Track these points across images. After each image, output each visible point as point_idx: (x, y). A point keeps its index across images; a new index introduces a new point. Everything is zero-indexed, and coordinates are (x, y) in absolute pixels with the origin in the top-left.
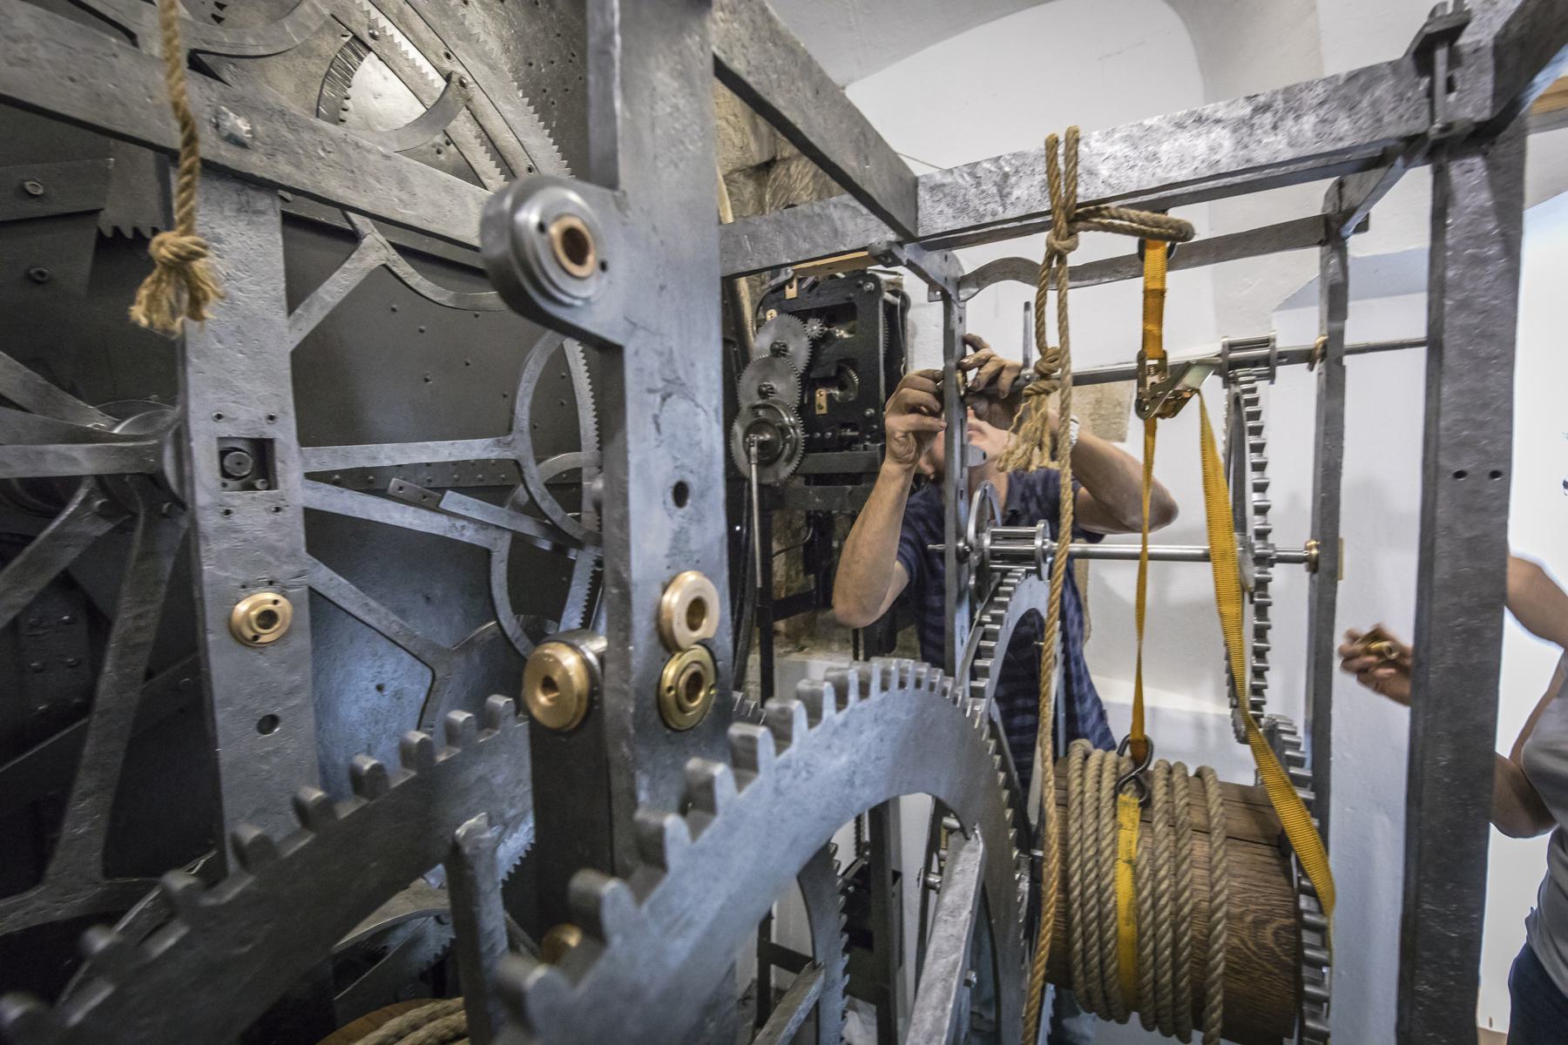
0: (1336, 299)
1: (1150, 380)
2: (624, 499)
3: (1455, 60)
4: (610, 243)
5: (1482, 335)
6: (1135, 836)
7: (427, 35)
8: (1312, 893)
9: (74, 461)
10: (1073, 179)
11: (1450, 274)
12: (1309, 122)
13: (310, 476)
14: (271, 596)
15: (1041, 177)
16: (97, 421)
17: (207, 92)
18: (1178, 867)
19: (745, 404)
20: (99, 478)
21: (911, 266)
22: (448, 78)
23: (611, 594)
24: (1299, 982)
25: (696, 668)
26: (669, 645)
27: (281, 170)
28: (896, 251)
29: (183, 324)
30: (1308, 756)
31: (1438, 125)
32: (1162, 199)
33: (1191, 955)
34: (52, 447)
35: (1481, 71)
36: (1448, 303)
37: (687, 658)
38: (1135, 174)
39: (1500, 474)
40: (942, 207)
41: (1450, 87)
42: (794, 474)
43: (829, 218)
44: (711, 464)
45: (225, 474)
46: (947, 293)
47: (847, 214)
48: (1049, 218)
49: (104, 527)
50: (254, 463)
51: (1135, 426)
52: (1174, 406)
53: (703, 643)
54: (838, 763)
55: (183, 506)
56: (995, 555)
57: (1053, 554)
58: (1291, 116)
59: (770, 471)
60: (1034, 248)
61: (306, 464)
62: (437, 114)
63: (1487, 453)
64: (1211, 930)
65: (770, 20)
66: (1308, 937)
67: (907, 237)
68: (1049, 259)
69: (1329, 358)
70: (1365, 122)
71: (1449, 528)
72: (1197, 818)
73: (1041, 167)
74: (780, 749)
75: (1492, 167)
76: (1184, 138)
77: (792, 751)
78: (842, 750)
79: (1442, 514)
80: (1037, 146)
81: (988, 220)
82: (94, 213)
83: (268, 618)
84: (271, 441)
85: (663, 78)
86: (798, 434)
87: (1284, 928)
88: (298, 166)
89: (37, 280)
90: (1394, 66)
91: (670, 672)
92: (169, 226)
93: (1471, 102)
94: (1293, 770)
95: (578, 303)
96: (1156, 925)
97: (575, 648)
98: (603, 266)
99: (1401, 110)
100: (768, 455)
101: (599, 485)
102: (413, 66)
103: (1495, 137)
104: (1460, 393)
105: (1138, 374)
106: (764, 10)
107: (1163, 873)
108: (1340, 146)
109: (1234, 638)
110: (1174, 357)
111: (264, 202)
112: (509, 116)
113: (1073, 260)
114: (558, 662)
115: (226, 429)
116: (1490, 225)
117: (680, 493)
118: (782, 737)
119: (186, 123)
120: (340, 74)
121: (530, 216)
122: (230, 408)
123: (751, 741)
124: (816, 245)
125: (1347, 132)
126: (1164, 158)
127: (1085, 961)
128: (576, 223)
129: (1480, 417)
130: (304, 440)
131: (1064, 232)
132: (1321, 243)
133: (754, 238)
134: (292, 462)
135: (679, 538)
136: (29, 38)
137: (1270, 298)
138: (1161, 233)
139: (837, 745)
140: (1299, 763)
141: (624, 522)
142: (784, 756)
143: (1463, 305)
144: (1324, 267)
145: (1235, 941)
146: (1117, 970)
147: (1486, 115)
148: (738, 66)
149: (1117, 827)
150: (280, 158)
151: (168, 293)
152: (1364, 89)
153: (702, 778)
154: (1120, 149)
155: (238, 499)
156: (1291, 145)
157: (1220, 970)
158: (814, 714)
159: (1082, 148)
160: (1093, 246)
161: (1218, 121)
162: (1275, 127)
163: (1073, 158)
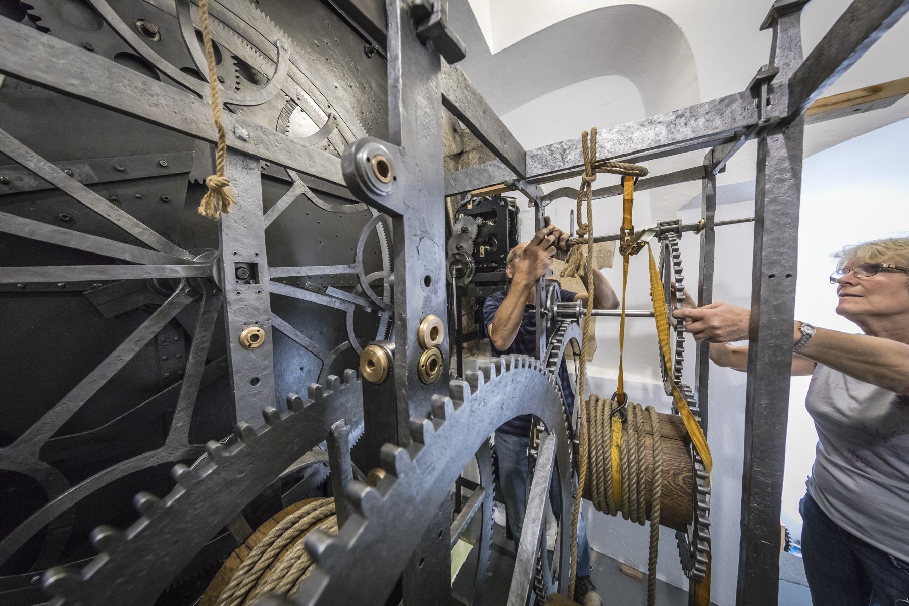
0: (710, 202)
1: (626, 238)
2: (404, 282)
3: (770, 90)
4: (397, 168)
5: (782, 214)
6: (620, 436)
7: (321, 98)
8: (701, 462)
9: (176, 271)
10: (594, 150)
11: (767, 187)
12: (702, 121)
13: (272, 279)
14: (257, 328)
15: (580, 150)
16: (187, 256)
17: (230, 118)
18: (639, 449)
19: (450, 253)
20: (187, 279)
21: (523, 191)
22: (329, 116)
23: (397, 326)
24: (696, 502)
25: (434, 357)
26: (422, 347)
27: (261, 151)
28: (516, 183)
29: (220, 214)
30: (698, 402)
31: (763, 120)
32: (636, 157)
33: (645, 488)
34: (168, 266)
35: (783, 95)
36: (766, 199)
37: (430, 353)
38: (622, 147)
39: (791, 276)
40: (537, 164)
41: (768, 103)
42: (471, 282)
43: (488, 170)
44: (440, 269)
45: (238, 277)
46: (536, 203)
47: (495, 169)
48: (583, 168)
49: (189, 300)
50: (249, 273)
51: (618, 259)
52: (638, 249)
53: (437, 346)
54: (495, 400)
55: (221, 291)
57: (585, 314)
58: (694, 118)
60: (575, 183)
61: (271, 273)
62: (325, 131)
63: (784, 266)
65: (465, 80)
66: (699, 481)
67: (521, 177)
68: (583, 186)
69: (706, 229)
71: (766, 300)
72: (647, 428)
73: (580, 145)
74: (473, 392)
75: (787, 138)
76: (644, 130)
77: (478, 392)
78: (499, 394)
79: (763, 293)
80: (578, 137)
81: (557, 169)
82: (188, 173)
83: (255, 337)
84: (257, 264)
85: (420, 99)
87: (687, 477)
88: (267, 150)
89: (164, 201)
90: (742, 95)
91: (423, 358)
92: (215, 173)
93: (778, 109)
94: (691, 408)
95: (384, 194)
96: (629, 474)
97: (382, 348)
98: (395, 179)
99: (745, 114)
100: (460, 274)
101: (392, 278)
102: (315, 111)
103: (788, 124)
104: (772, 240)
105: (621, 238)
106: (463, 75)
107: (632, 451)
108: (716, 131)
109: (665, 350)
110: (637, 230)
111: (253, 164)
112: (354, 131)
113: (595, 186)
114: (375, 353)
115: (238, 259)
116: (786, 164)
117: (427, 281)
118: (474, 387)
119: (220, 129)
120: (286, 114)
121: (363, 155)
122: (239, 250)
123: (461, 387)
124: (482, 182)
125: (719, 125)
126: (635, 139)
127: (598, 489)
128: (383, 159)
130: (271, 263)
131: (590, 173)
132: (703, 178)
133: (455, 180)
134: (266, 273)
135: (427, 300)
136: (158, 95)
137: (681, 202)
138: (632, 174)
139: (495, 392)
140: (694, 405)
141: (403, 292)
142: (474, 395)
143: (773, 201)
144: (704, 188)
145: (665, 482)
146: (612, 493)
147: (785, 114)
148: (451, 98)
149: (612, 431)
150: (260, 146)
151: (213, 201)
152: (727, 106)
153: (439, 404)
154: (615, 136)
155: (243, 287)
156: (693, 132)
158: (487, 377)
159: (598, 136)
160: (603, 180)
161: (659, 123)
162: (686, 124)
163: (594, 141)
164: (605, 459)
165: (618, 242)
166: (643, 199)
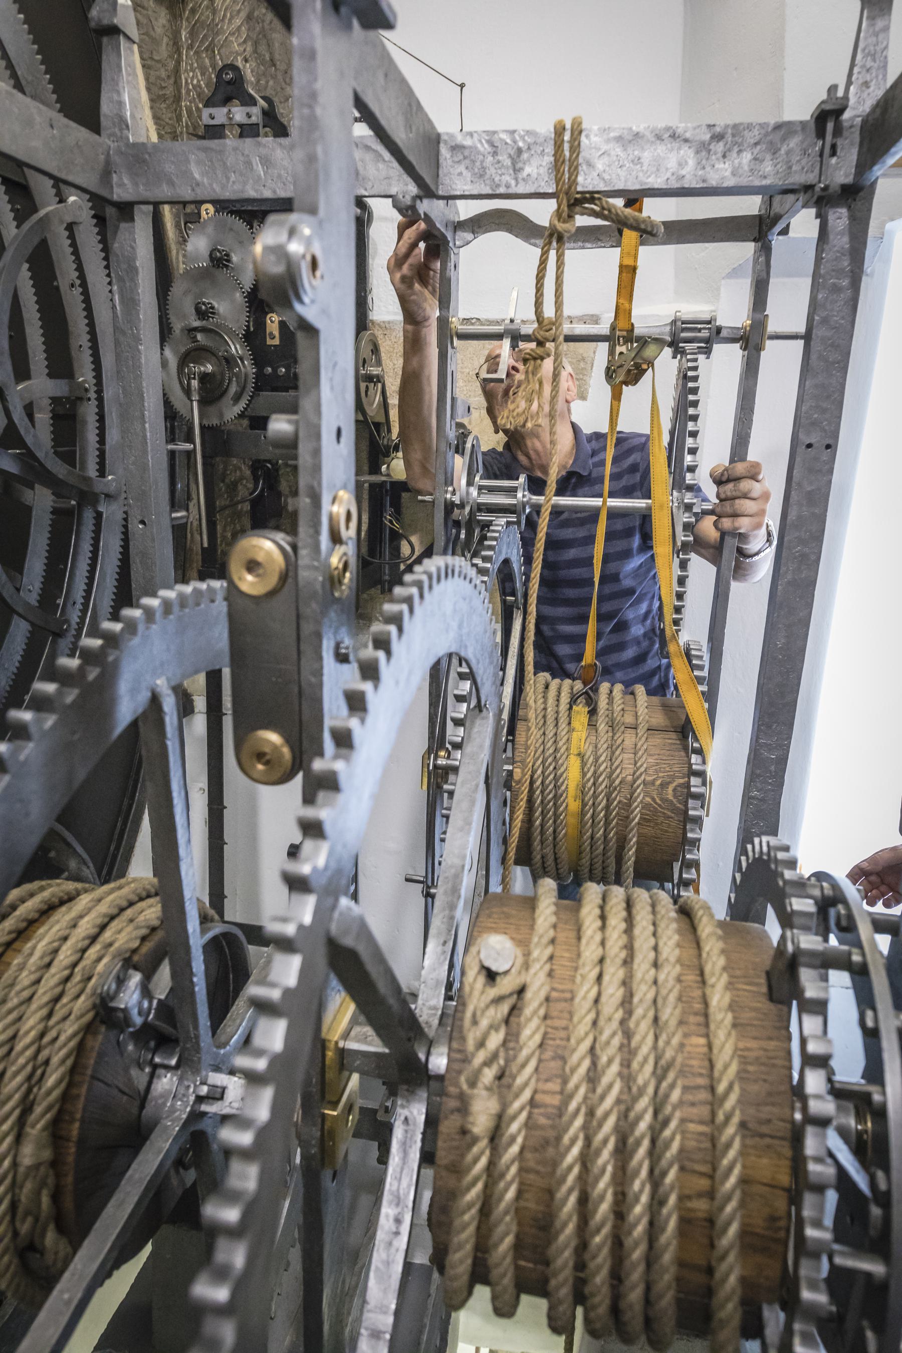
3: (838, 131)
6: (584, 735)
10: (574, 170)
12: (747, 157)
18: (613, 753)
19: (178, 327)
33: (617, 814)
35: (852, 144)
36: (817, 318)
40: (461, 168)
42: (242, 416)
47: (368, 157)
56: (481, 508)
59: (212, 409)
63: (825, 431)
64: (632, 794)
70: (781, 167)
72: (629, 719)
73: (550, 149)
75: (852, 218)
76: (661, 149)
80: (546, 129)
81: (502, 190)
86: (248, 367)
87: (680, 785)
90: (803, 124)
93: (841, 171)
94: (696, 673)
96: (595, 796)
99: (804, 162)
100: (211, 392)
103: (855, 195)
104: (816, 386)
105: (610, 338)
107: (602, 758)
114: (261, 548)
116: (846, 263)
127: (542, 833)
129: (825, 405)
131: (565, 215)
132: (755, 240)
140: (701, 668)
145: (648, 799)
146: (566, 834)
149: (571, 730)
152: (784, 139)
156: (733, 174)
157: (636, 820)
161: (686, 141)
162: (724, 156)
163: (576, 147)
164: (556, 779)
165: (604, 347)
166: (654, 259)
